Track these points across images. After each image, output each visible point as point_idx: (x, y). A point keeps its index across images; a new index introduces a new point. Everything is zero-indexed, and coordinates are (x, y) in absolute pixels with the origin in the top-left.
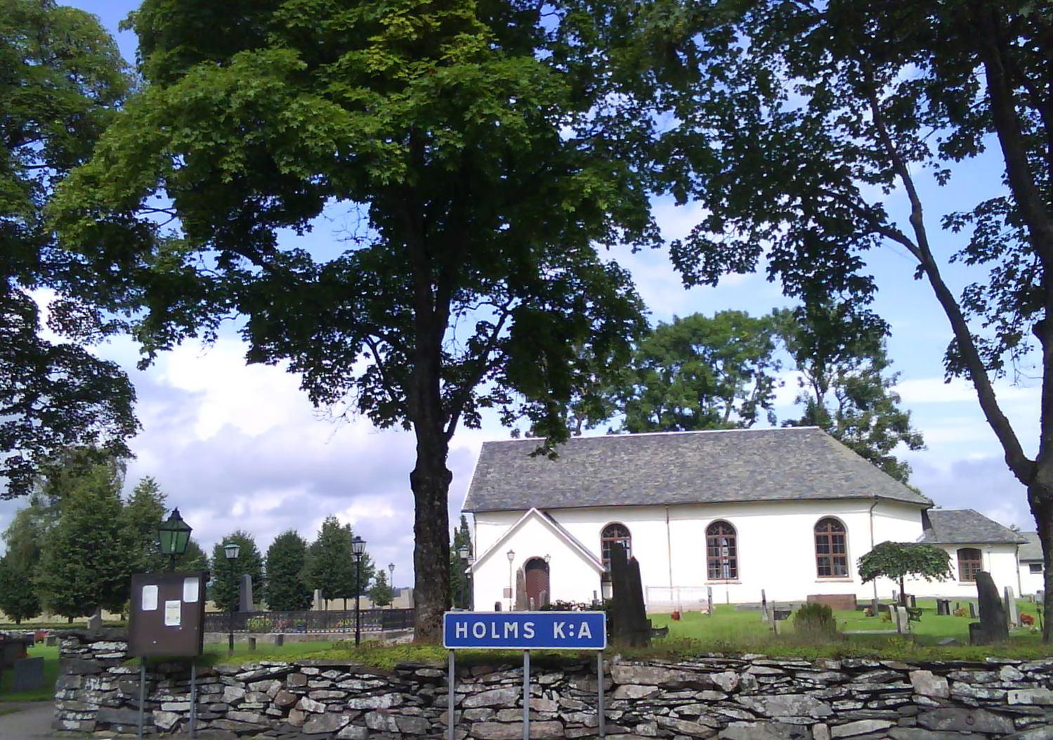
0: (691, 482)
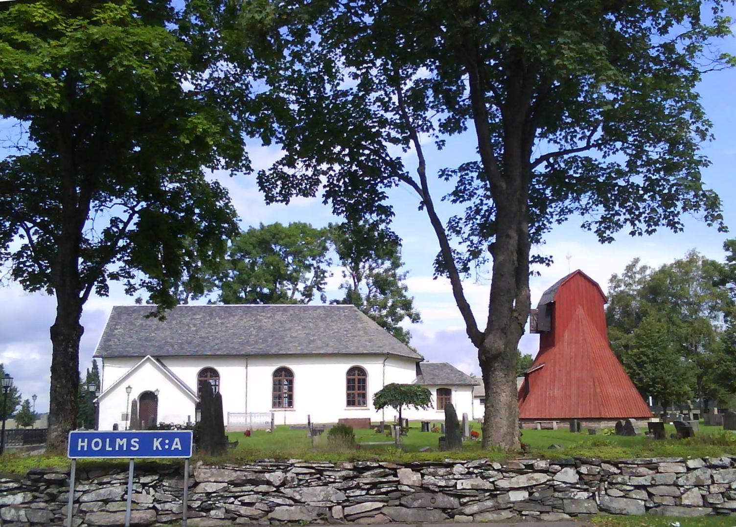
0: (265, 340)
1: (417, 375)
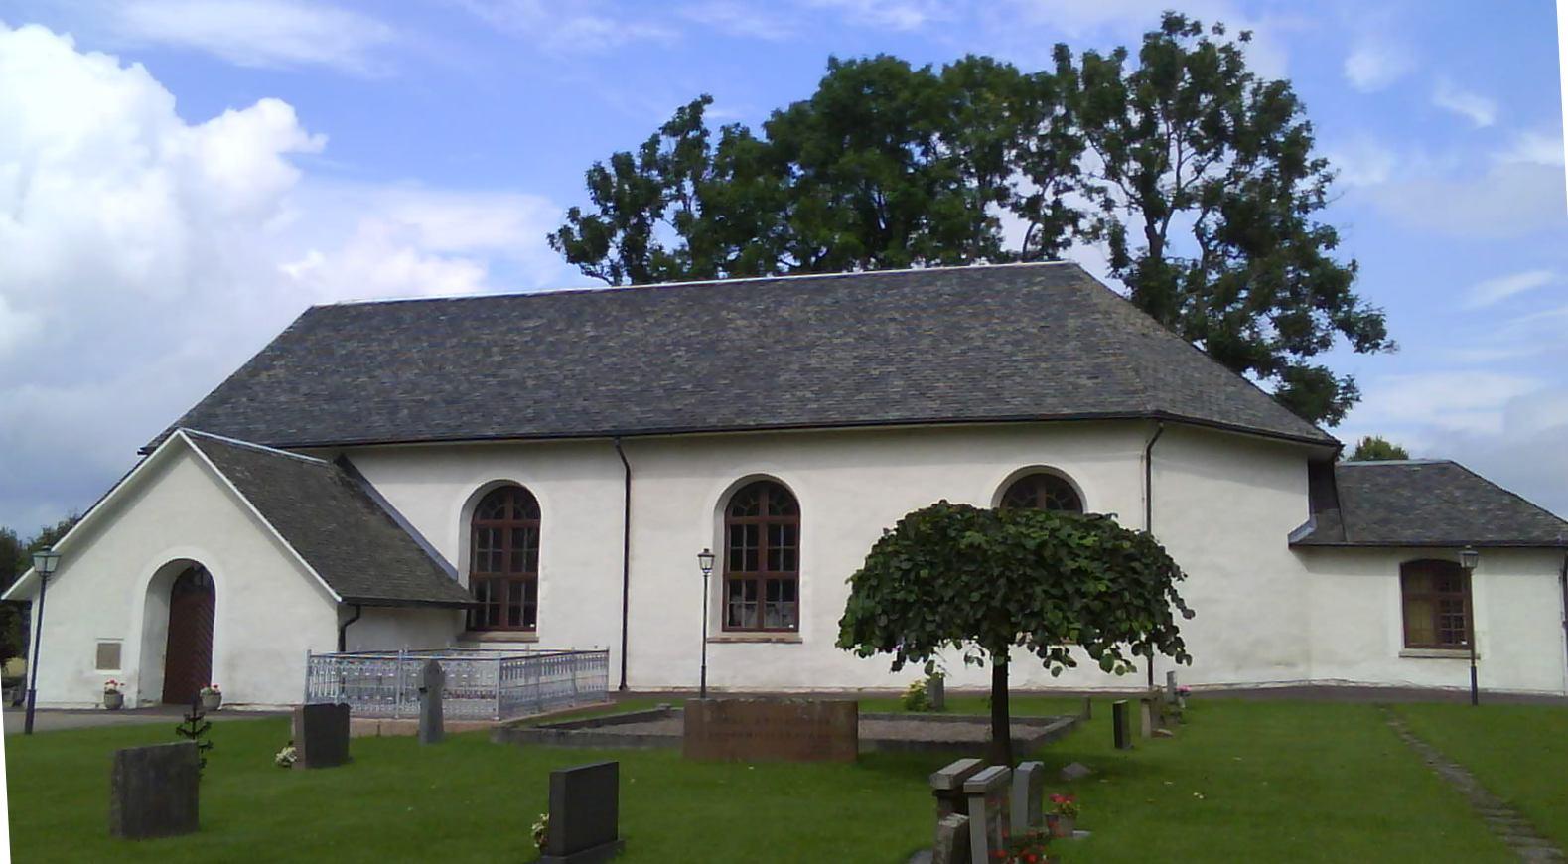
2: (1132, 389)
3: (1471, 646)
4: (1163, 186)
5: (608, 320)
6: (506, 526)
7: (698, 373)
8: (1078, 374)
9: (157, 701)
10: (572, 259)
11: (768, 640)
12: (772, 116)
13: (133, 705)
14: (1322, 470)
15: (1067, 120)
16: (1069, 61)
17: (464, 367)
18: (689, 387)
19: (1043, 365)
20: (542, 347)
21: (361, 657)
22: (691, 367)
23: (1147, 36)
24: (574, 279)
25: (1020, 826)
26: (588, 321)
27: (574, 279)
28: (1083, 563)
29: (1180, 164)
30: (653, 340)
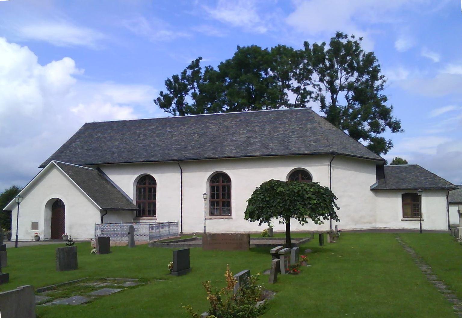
1: (378, 178)
2: (326, 145)
3: (421, 217)
4: (336, 84)
5: (174, 126)
6: (146, 187)
7: (201, 142)
8: (310, 141)
9: (49, 239)
10: (161, 107)
11: (223, 218)
12: (220, 64)
13: (43, 240)
14: (380, 168)
15: (308, 64)
16: (309, 47)
17: (132, 141)
18: (199, 146)
19: (301, 139)
20: (155, 135)
21: (108, 224)
22: (199, 140)
23: (332, 39)
24: (162, 114)
25: (293, 262)
26: (168, 127)
27: (162, 114)
28: (310, 195)
29: (341, 77)
30: (187, 132)
